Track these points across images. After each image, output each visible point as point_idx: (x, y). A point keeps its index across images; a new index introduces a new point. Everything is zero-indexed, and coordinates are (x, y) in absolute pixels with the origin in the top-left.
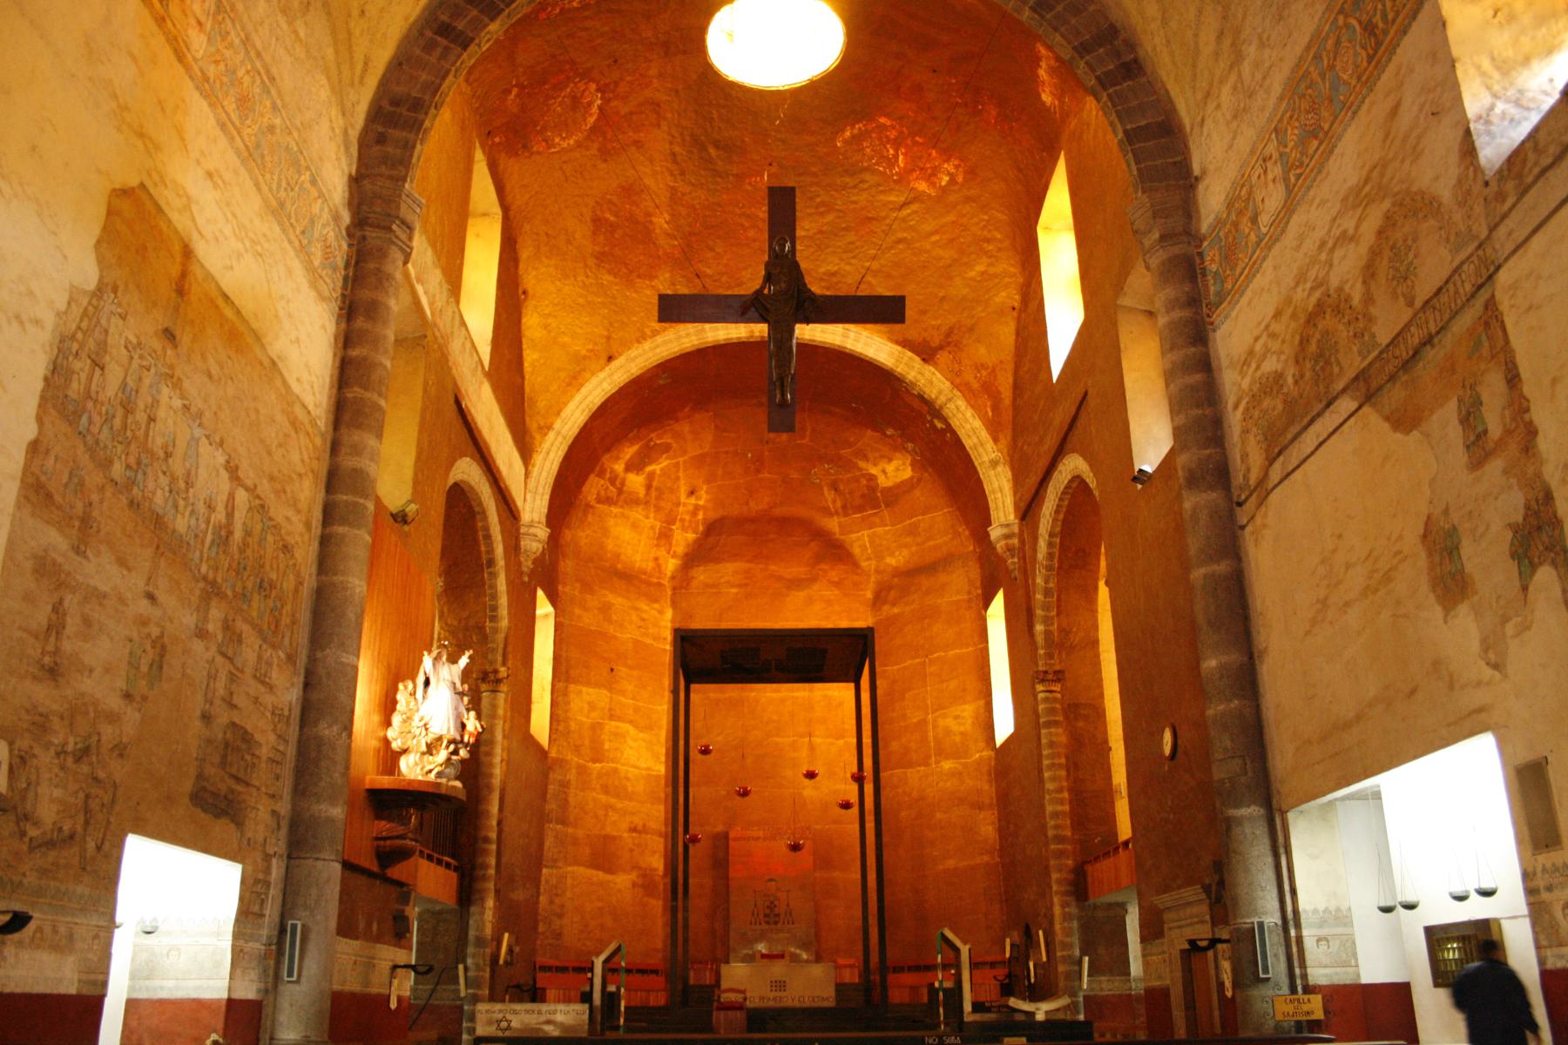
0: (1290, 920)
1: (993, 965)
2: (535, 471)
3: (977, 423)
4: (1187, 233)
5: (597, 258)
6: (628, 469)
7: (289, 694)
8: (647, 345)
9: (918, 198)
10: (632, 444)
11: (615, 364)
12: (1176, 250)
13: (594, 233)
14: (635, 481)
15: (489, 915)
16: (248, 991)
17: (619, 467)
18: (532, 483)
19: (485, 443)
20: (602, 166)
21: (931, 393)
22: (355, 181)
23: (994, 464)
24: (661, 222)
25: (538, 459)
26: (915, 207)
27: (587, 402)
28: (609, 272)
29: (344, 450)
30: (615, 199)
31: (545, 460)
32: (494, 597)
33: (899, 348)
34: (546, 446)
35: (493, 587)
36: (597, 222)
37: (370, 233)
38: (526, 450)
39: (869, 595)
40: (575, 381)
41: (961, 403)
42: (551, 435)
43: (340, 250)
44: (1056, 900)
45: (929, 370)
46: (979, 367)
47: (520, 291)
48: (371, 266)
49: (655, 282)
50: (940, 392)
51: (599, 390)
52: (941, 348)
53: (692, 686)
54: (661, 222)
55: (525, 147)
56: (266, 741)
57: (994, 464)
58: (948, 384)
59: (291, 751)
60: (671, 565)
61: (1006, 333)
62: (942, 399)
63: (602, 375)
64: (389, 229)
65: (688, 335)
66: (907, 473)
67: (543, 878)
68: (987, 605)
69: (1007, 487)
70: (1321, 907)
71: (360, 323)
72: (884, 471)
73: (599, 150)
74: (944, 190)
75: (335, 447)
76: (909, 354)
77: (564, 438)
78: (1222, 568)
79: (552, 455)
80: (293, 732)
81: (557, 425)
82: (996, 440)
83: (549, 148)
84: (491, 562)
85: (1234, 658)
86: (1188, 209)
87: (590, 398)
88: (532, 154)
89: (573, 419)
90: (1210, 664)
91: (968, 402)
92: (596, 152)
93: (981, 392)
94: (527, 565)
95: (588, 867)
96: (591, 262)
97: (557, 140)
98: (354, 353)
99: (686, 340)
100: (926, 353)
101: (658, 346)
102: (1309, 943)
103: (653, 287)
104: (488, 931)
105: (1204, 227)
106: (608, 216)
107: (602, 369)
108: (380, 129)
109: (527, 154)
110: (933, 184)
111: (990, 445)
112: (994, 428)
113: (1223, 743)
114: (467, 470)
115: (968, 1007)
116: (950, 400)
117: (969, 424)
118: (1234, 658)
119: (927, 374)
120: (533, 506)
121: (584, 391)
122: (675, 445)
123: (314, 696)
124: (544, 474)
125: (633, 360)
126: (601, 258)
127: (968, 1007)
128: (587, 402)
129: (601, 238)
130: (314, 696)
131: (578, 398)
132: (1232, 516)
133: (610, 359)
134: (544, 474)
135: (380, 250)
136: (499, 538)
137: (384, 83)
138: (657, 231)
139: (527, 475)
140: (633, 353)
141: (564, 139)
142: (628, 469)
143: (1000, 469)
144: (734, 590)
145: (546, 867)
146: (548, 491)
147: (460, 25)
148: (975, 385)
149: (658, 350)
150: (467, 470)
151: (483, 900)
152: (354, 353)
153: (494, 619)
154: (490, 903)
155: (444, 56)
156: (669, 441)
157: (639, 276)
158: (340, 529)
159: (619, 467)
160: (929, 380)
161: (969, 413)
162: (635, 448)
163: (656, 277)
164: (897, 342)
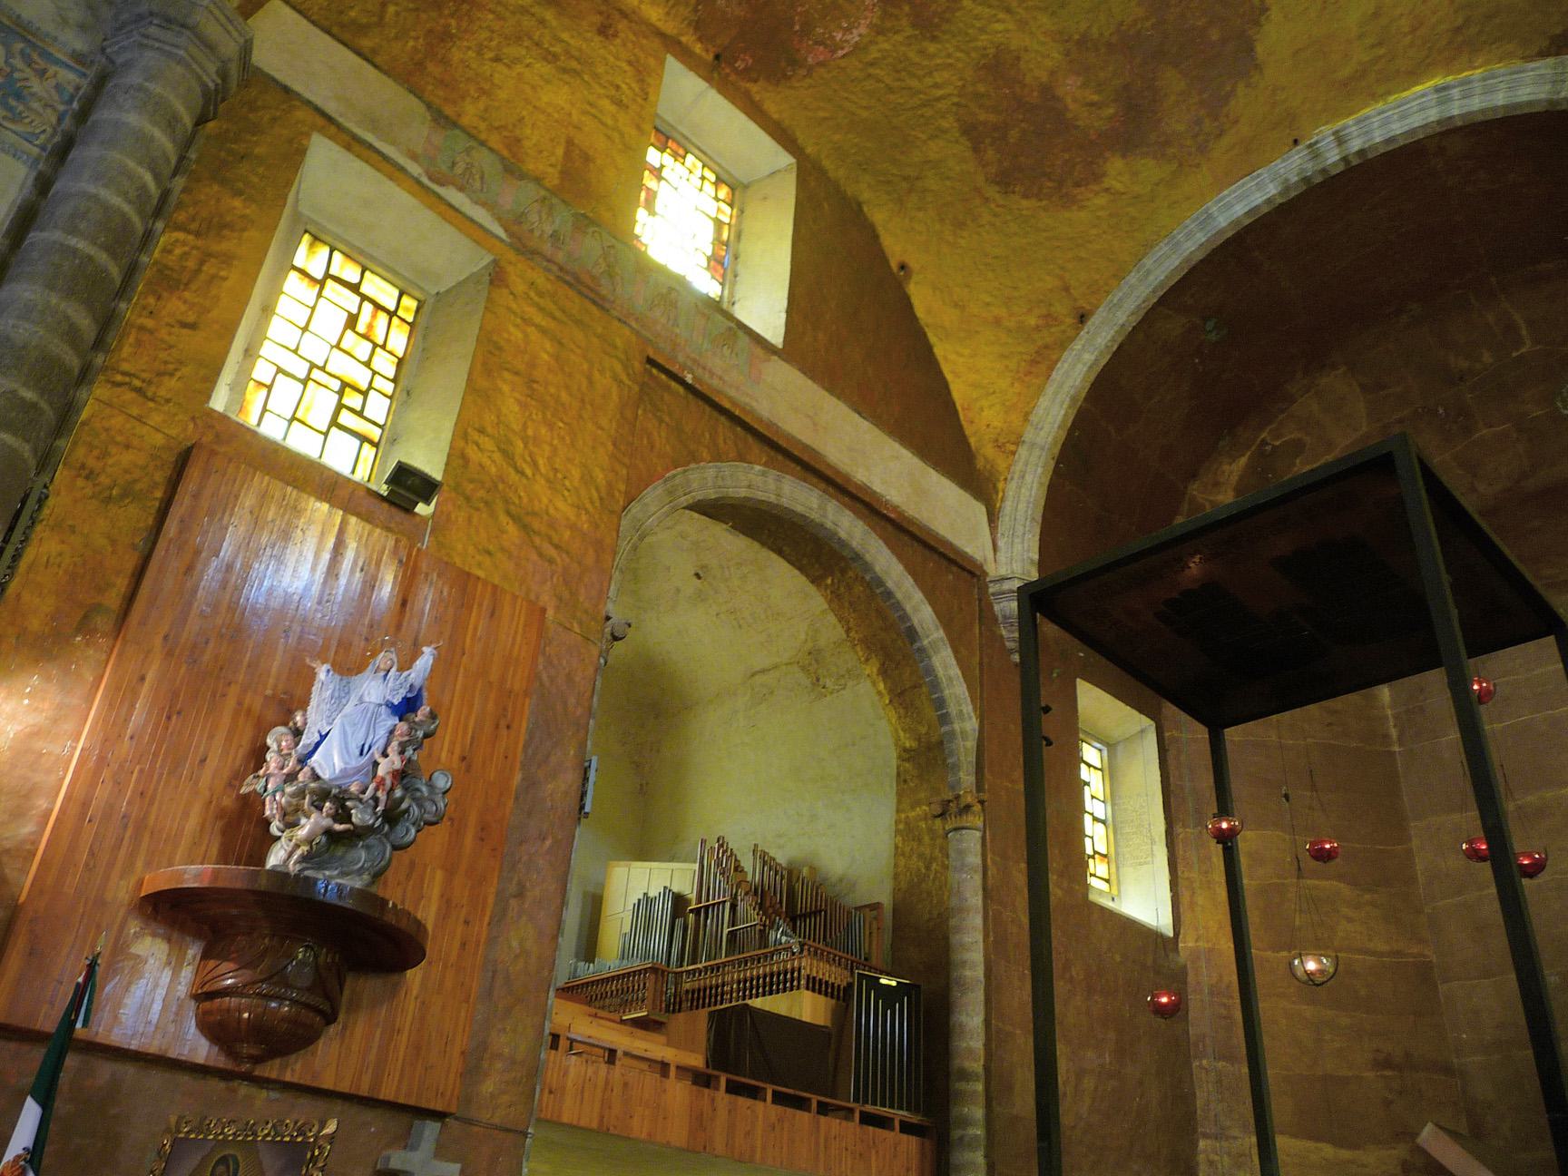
5: (998, 183)
8: (1132, 278)
10: (1234, 459)
13: (976, 150)
18: (1004, 523)
19: (806, 447)
20: (932, 48)
24: (1072, 90)
27: (1066, 388)
28: (1025, 196)
30: (981, 88)
31: (1019, 487)
33: (1551, 61)
34: (1018, 468)
36: (970, 131)
47: (894, 265)
49: (1107, 182)
51: (1080, 366)
53: (1232, 734)
55: (794, 63)
63: (1077, 345)
65: (1189, 236)
67: (1201, 1158)
73: (914, 26)
77: (1042, 449)
79: (1029, 478)
83: (833, 52)
87: (1070, 382)
88: (810, 69)
89: (1050, 419)
92: (909, 31)
95: (1295, 1136)
96: (992, 192)
97: (838, 36)
99: (1189, 244)
101: (1149, 272)
103: (1107, 190)
106: (982, 117)
109: (803, 72)
122: (1308, 439)
124: (1022, 506)
125: (1119, 305)
126: (1005, 181)
128: (1066, 388)
129: (990, 154)
131: (1050, 390)
133: (1082, 318)
134: (1022, 506)
136: (918, 596)
138: (1071, 106)
139: (993, 518)
141: (848, 30)
145: (1206, 1136)
149: (1151, 278)
156: (1296, 435)
157: (1078, 185)
162: (1243, 461)
163: (1104, 175)
164: (1543, 54)
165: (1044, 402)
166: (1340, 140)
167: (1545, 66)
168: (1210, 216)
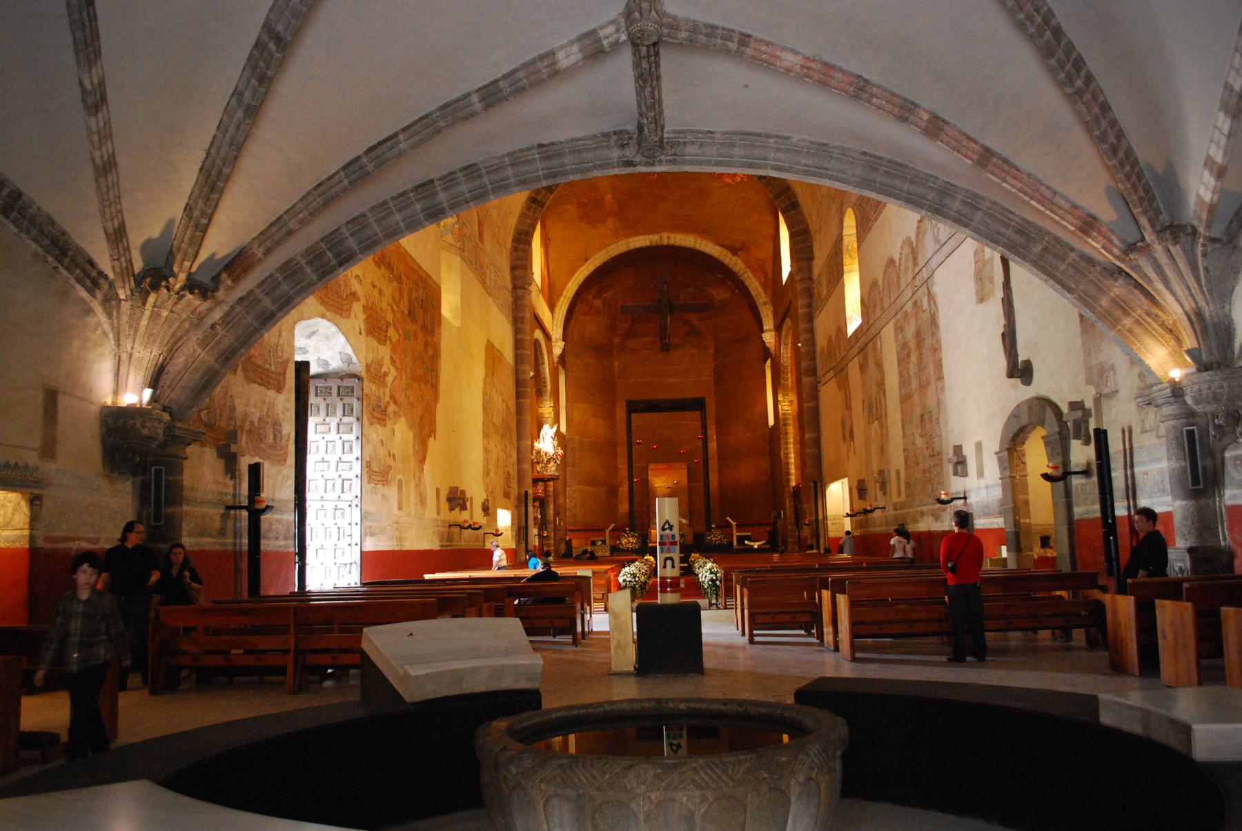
0: (825, 518)
1: (768, 524)
2: (556, 315)
3: (757, 284)
4: (811, 279)
6: (594, 298)
7: (515, 456)
8: (603, 252)
9: (727, 185)
11: (589, 262)
12: (805, 285)
14: (598, 303)
15: (551, 512)
16: (514, 546)
17: (590, 298)
21: (736, 269)
22: (513, 269)
23: (765, 303)
24: (608, 197)
25: (557, 310)
26: (726, 189)
29: (519, 373)
32: (545, 378)
35: (544, 373)
37: (518, 291)
38: (552, 308)
39: (712, 352)
40: (572, 273)
41: (750, 274)
42: (562, 298)
43: (510, 299)
44: (787, 499)
45: (735, 258)
46: (758, 260)
48: (520, 303)
50: (741, 269)
52: (740, 249)
53: (634, 416)
54: (608, 197)
56: (511, 470)
57: (765, 303)
58: (744, 265)
59: (516, 474)
60: (617, 340)
61: (769, 246)
62: (742, 272)
63: (583, 268)
64: (524, 288)
66: (728, 295)
68: (765, 363)
69: (771, 315)
70: (834, 514)
71: (519, 325)
72: (718, 293)
74: (738, 183)
75: (517, 371)
76: (725, 251)
78: (812, 404)
80: (516, 468)
81: (564, 293)
82: (766, 293)
84: (543, 363)
85: (814, 435)
86: (810, 269)
90: (807, 436)
91: (753, 273)
93: (758, 269)
94: (556, 360)
98: (519, 337)
100: (734, 251)
102: (829, 525)
104: (552, 519)
105: (815, 278)
107: (583, 265)
108: (515, 245)
110: (733, 180)
111: (763, 295)
112: (765, 287)
113: (809, 462)
114: (538, 334)
115: (735, 543)
116: (744, 273)
117: (754, 285)
118: (814, 435)
119: (735, 260)
120: (556, 332)
121: (576, 275)
123: (521, 456)
127: (735, 543)
130: (521, 456)
131: (573, 280)
132: (816, 386)
133: (587, 260)
135: (523, 296)
137: (515, 229)
140: (597, 256)
142: (594, 298)
143: (768, 306)
144: (647, 351)
146: (562, 324)
147: (539, 198)
148: (756, 267)
150: (538, 334)
151: (549, 506)
152: (519, 337)
153: (545, 386)
154: (552, 506)
155: (534, 212)
158: (521, 400)
159: (590, 298)
160: (736, 263)
161: (753, 279)
164: (720, 245)
165: (570, 283)
166: (668, 238)
167: (719, 248)
168: (629, 243)
